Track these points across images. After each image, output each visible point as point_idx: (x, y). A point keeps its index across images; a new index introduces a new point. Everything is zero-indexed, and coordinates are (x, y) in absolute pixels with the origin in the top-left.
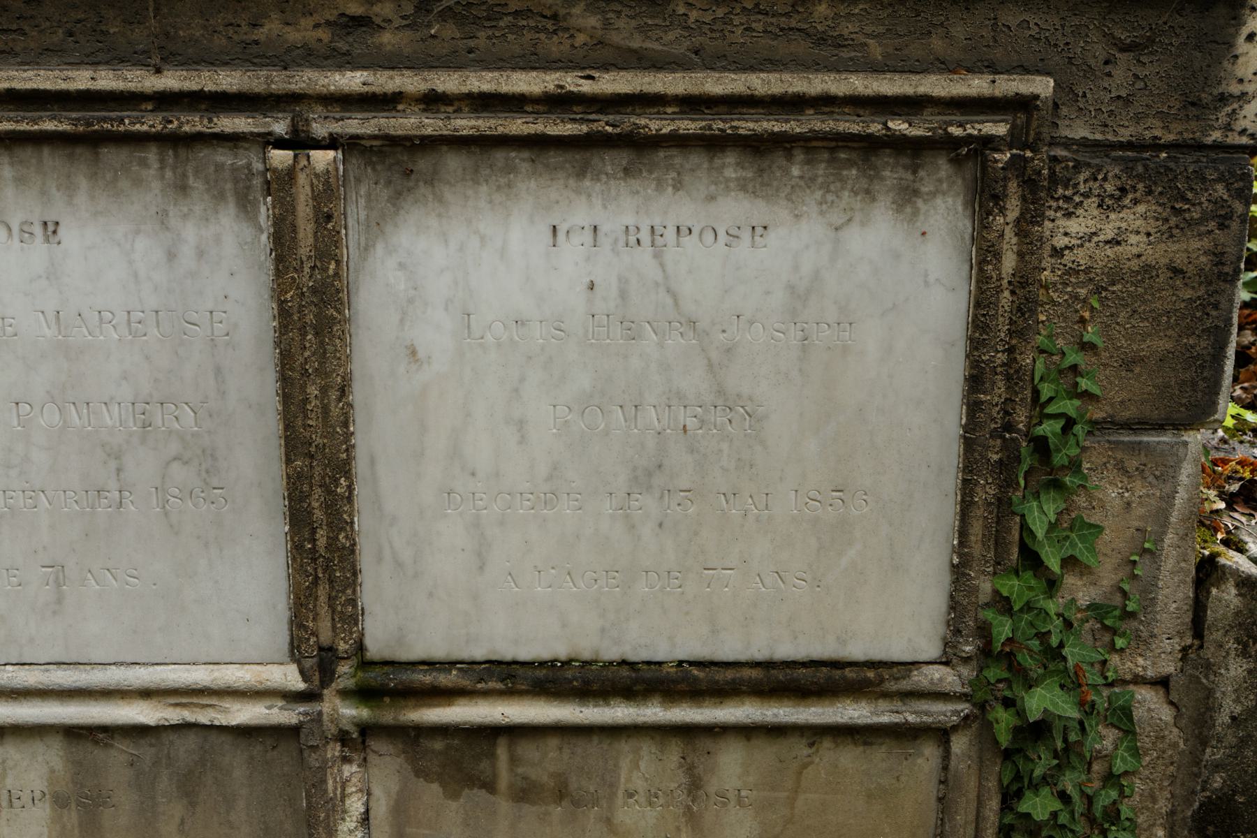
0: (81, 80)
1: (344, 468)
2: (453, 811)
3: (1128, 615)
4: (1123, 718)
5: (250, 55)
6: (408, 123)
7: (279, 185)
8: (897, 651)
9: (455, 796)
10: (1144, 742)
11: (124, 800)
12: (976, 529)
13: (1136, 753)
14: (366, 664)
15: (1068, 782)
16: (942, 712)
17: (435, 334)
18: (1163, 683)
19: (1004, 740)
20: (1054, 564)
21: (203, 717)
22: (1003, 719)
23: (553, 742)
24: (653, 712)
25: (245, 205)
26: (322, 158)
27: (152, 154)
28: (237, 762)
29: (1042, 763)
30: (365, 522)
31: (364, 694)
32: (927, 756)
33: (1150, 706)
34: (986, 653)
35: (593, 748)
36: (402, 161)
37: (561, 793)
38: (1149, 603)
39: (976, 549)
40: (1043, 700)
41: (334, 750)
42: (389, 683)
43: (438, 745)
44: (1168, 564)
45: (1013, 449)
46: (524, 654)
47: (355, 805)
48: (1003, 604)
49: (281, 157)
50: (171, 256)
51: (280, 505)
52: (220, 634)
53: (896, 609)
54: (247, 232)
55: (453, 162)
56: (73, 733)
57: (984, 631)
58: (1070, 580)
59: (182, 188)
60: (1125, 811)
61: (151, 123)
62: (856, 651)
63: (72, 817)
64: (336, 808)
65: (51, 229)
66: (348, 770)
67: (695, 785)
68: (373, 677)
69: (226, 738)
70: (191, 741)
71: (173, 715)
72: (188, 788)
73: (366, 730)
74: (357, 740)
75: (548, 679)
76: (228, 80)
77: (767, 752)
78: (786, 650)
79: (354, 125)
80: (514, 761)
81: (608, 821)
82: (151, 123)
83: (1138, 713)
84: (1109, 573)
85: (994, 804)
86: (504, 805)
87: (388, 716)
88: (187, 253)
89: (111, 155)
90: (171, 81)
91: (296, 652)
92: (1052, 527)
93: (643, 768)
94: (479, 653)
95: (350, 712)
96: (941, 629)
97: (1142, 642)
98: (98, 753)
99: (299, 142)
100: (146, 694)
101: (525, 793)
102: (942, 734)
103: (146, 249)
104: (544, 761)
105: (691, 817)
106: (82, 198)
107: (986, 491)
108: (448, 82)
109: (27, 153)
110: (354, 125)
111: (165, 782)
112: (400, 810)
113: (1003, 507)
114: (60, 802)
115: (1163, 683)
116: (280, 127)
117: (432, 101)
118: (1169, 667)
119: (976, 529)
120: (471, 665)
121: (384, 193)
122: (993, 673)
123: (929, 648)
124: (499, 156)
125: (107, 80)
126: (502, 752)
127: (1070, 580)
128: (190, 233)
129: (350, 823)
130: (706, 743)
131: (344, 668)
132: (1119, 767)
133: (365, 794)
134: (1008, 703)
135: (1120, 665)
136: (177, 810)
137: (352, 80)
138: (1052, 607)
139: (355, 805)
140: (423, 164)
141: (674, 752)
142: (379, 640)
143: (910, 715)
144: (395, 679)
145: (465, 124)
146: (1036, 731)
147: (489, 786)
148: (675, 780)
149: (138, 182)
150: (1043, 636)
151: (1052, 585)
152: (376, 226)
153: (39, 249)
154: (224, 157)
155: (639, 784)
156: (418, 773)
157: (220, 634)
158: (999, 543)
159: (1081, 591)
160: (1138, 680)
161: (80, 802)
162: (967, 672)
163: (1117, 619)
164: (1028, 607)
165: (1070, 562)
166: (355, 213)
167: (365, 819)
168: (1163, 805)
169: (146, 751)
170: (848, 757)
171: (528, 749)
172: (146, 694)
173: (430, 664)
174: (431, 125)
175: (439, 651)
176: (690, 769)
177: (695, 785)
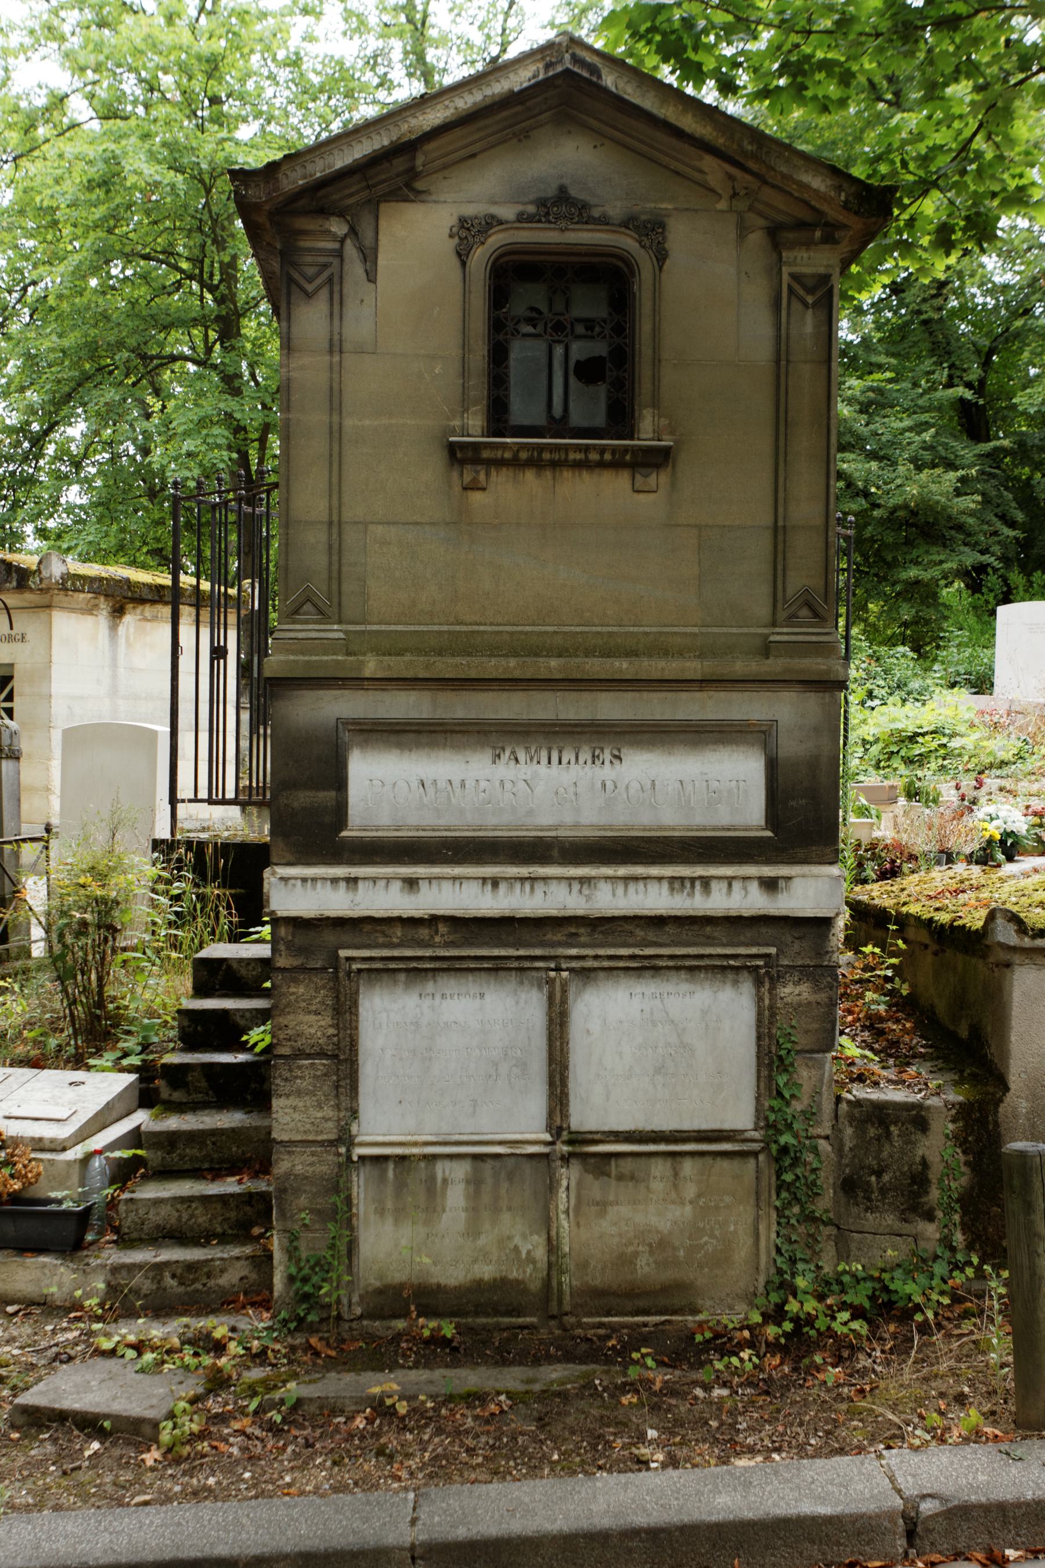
0: (496, 952)
1: (566, 1068)
2: (597, 1184)
3: (814, 1114)
4: (815, 1150)
5: (542, 944)
6: (590, 964)
7: (550, 982)
8: (739, 1126)
9: (597, 1179)
10: (823, 1158)
11: (489, 1181)
12: (762, 1085)
13: (820, 1162)
14: (570, 1133)
15: (798, 1171)
16: (756, 1146)
17: (595, 1026)
18: (827, 1138)
19: (774, 1152)
20: (787, 1096)
21: (518, 1151)
22: (774, 1147)
23: (629, 1160)
24: (662, 1147)
25: (540, 988)
26: (565, 974)
27: (513, 973)
28: (527, 1167)
29: (787, 1162)
30: (571, 1085)
31: (570, 1142)
32: (751, 1163)
33: (823, 1145)
34: (768, 1126)
35: (642, 1161)
36: (586, 975)
37: (632, 1178)
38: (820, 1109)
39: (763, 1091)
40: (785, 1139)
41: (559, 1163)
42: (578, 1139)
43: (592, 1161)
44: (825, 1096)
45: (773, 1059)
46: (621, 1128)
47: (564, 1183)
48: (772, 1109)
49: (552, 974)
50: (517, 1003)
51: (546, 1079)
52: (524, 1122)
53: (738, 1113)
54: (540, 995)
55: (601, 974)
56: (476, 1157)
57: (766, 1118)
58: (793, 1102)
59: (522, 983)
60: (819, 1183)
61: (515, 964)
62: (727, 1126)
63: (472, 1188)
64: (559, 1182)
65: (482, 995)
66: (563, 1170)
67: (676, 1174)
68: (573, 1136)
69: (524, 1159)
70: (513, 1160)
71: (509, 1151)
72: (510, 1177)
73: (571, 1155)
74: (566, 1159)
75: (629, 1137)
76: (538, 952)
77: (699, 1162)
78: (704, 1126)
79: (574, 964)
80: (617, 1166)
81: (648, 1188)
82: (515, 964)
83: (820, 1148)
84: (806, 1101)
85: (774, 1178)
86: (613, 1182)
87: (579, 1149)
88: (522, 1001)
89: (501, 973)
90: (521, 952)
91: (549, 1128)
92: (786, 1084)
93: (659, 1169)
94: (606, 1129)
95: (566, 1149)
96: (753, 1119)
97: (819, 1123)
98: (482, 1164)
99: (558, 969)
100: (500, 1143)
101: (620, 1178)
102: (755, 1154)
103: (510, 1001)
104: (627, 1165)
105: (675, 1186)
106: (492, 986)
107: (765, 1073)
108: (601, 952)
109: (477, 973)
110: (574, 964)
111: (503, 1175)
112: (580, 1184)
113: (770, 1078)
114: (468, 1182)
115: (827, 1138)
116: (553, 965)
117: (596, 957)
118: (828, 1132)
119: (762, 1085)
120: (604, 1133)
121: (580, 984)
122: (771, 1132)
123: (751, 1126)
124: (615, 972)
125: (503, 952)
126: (613, 1163)
127: (793, 1102)
128: (523, 996)
129: (563, 1189)
130: (679, 1159)
131: (565, 1133)
132: (814, 1166)
133: (568, 1176)
134: (776, 1142)
135: (812, 1131)
136: (505, 1185)
137: (574, 952)
138: (788, 1111)
139: (564, 1183)
140: (592, 975)
141: (669, 1162)
142: (574, 1126)
143: (745, 1147)
144: (580, 1137)
145: (606, 964)
146: (784, 1150)
147: (609, 1176)
148: (669, 1173)
149: (509, 981)
150: (786, 1120)
151: (788, 1104)
152: (578, 993)
153: (478, 1001)
154: (534, 974)
155: (658, 1174)
156: (586, 1171)
157: (524, 1122)
158: (770, 1090)
159: (797, 1106)
160: (819, 1137)
161: (475, 1183)
162: (762, 1132)
163: (810, 1115)
164: (780, 1110)
165: (793, 1096)
166: (572, 990)
167: (568, 1188)
168: (831, 1181)
169: (497, 1164)
170: (725, 1164)
171: (622, 1162)
172: (500, 1143)
173: (591, 1132)
174: (596, 964)
175: (594, 1128)
176: (674, 1169)
177: (676, 1174)
